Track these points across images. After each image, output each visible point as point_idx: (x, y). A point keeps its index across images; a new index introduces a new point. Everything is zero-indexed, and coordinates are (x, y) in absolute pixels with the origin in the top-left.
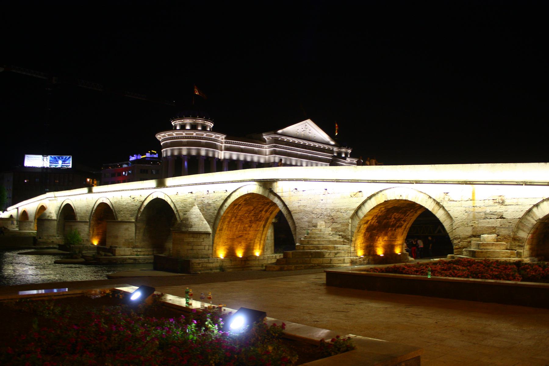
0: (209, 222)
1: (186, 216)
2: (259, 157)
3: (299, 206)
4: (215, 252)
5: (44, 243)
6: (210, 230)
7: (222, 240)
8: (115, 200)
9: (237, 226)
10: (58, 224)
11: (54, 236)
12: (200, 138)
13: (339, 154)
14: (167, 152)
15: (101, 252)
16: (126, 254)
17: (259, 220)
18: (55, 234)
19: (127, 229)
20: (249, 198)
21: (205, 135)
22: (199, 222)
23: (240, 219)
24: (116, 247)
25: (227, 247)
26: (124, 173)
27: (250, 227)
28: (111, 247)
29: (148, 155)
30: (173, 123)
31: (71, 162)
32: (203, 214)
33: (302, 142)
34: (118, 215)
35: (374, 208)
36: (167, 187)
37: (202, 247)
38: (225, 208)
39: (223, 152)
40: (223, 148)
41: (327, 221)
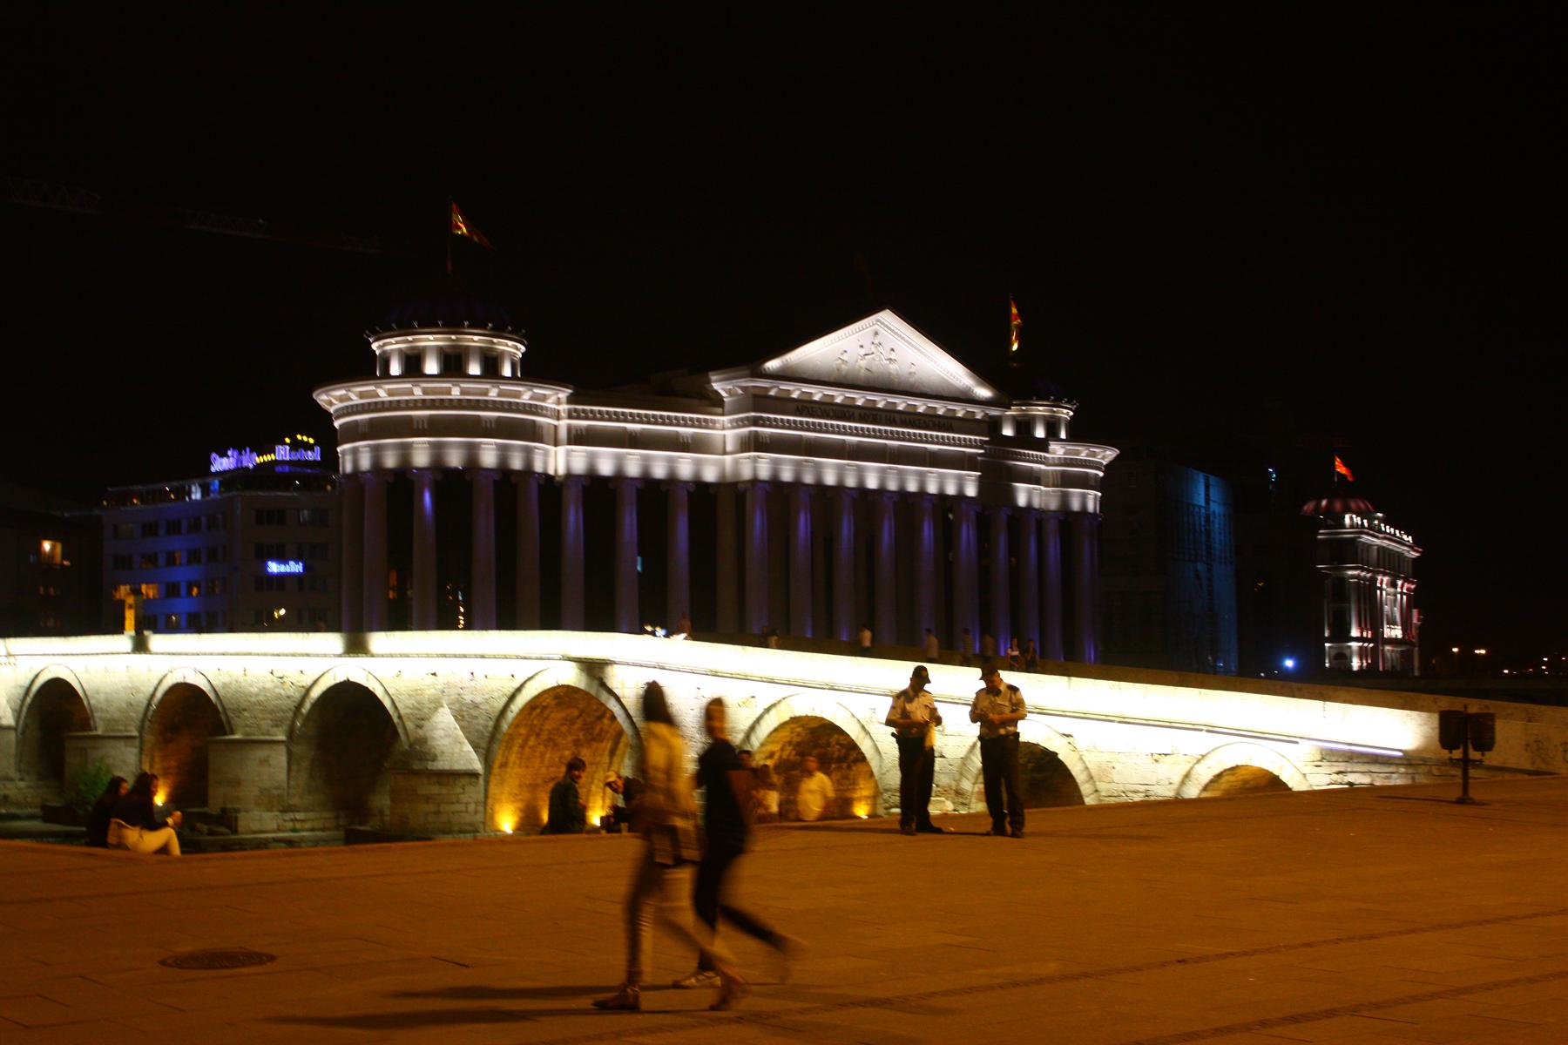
0: (476, 747)
1: (420, 732)
2: (698, 463)
4: (492, 818)
6: (478, 766)
7: (507, 789)
8: (226, 680)
9: (542, 755)
10: (19, 743)
13: (1024, 426)
14: (355, 456)
15: (199, 825)
17: (598, 738)
18: (13, 773)
19: (264, 761)
20: (561, 696)
21: (493, 394)
22: (453, 746)
23: (550, 739)
24: (237, 811)
25: (520, 805)
28: (224, 810)
29: (283, 453)
30: (374, 346)
32: (462, 728)
33: (860, 398)
34: (236, 721)
35: (776, 730)
37: (461, 807)
38: (510, 716)
39: (561, 450)
40: (563, 434)
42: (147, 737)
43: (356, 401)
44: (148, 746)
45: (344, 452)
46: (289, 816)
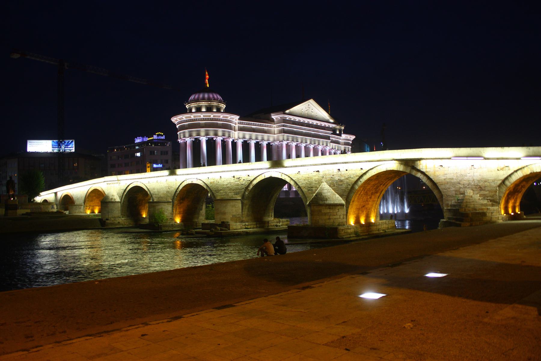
0: (341, 196)
2: (268, 136)
3: (444, 179)
5: (112, 224)
6: (343, 202)
8: (212, 181)
10: (122, 206)
11: (117, 216)
12: (217, 120)
16: (238, 228)
17: (377, 193)
23: (366, 192)
25: (355, 215)
26: (138, 154)
27: (371, 198)
29: (155, 137)
31: (74, 146)
33: (307, 121)
36: (286, 167)
39: (236, 133)
40: (237, 128)
41: (475, 189)
42: (176, 202)
43: (185, 119)
44: (175, 204)
45: (180, 134)
46: (244, 224)
